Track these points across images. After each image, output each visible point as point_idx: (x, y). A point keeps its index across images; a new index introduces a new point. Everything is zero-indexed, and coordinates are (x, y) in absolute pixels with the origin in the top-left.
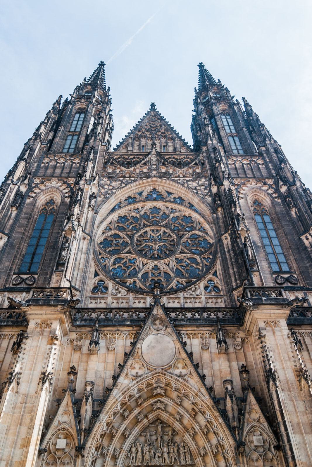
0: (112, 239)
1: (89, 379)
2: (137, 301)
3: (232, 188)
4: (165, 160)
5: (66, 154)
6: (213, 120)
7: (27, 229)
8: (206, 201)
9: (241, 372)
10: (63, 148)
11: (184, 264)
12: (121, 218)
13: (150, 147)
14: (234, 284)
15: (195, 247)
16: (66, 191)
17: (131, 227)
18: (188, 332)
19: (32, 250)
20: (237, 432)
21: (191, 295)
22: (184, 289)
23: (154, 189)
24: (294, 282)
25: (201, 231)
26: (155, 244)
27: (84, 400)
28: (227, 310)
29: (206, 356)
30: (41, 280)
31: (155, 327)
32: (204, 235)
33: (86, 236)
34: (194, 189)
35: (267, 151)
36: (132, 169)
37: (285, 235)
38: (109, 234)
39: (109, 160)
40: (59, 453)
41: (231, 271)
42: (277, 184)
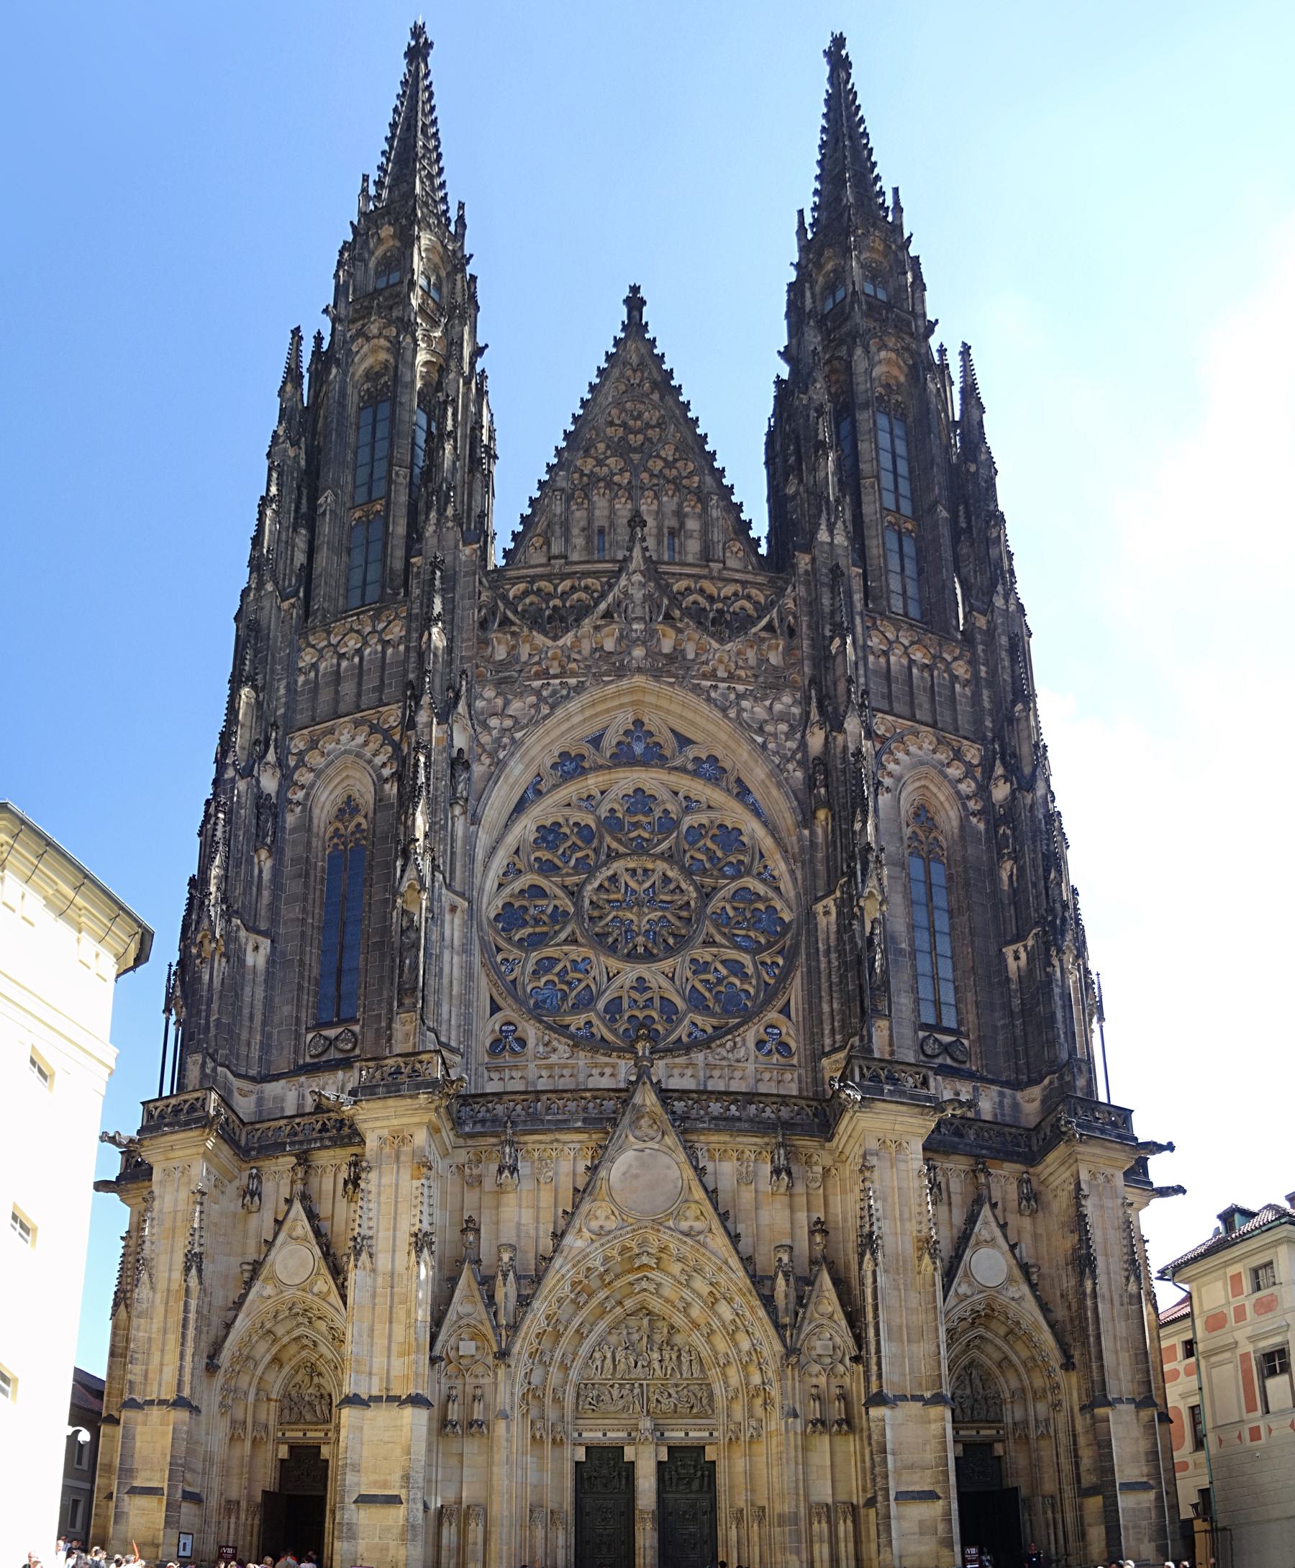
0: (525, 903)
1: (504, 1241)
2: (594, 1071)
9: (812, 1233)
12: (549, 835)
15: (741, 929)
20: (788, 1333)
21: (724, 1058)
25: (764, 881)
27: (500, 1277)
28: (803, 1103)
32: (771, 894)
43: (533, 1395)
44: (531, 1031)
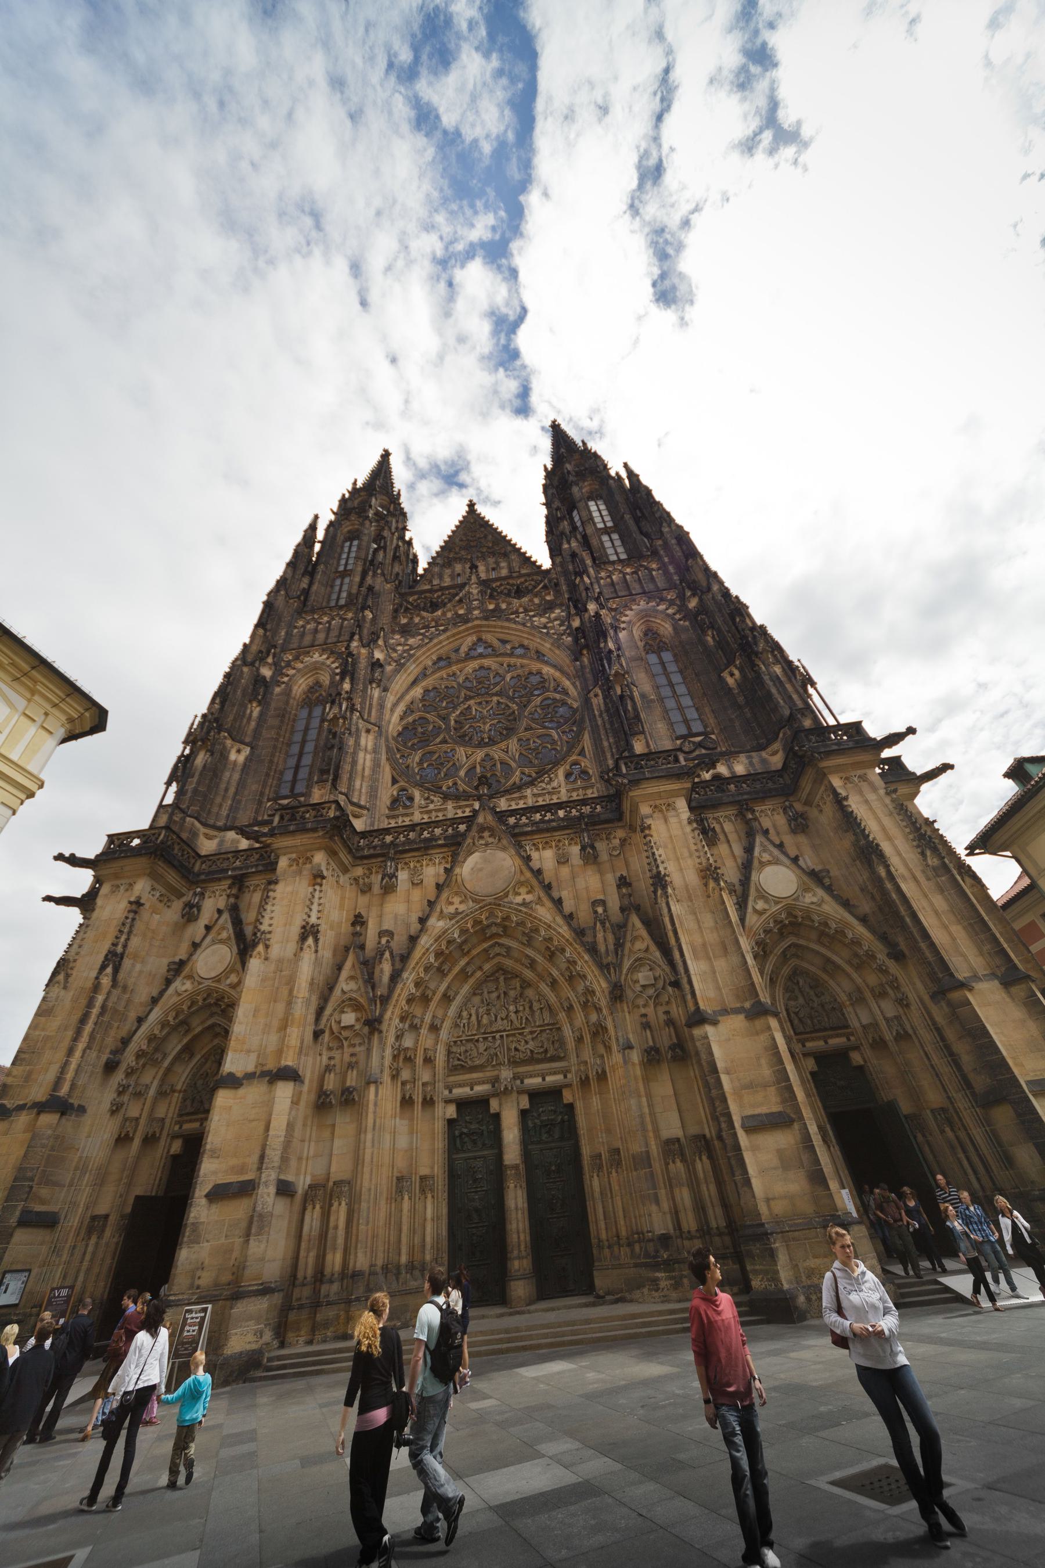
1: (385, 928)
2: (459, 811)
3: (603, 612)
4: (493, 590)
5: (331, 608)
6: (575, 513)
7: (282, 733)
9: (619, 887)
10: (329, 601)
11: (532, 746)
16: (337, 665)
17: (444, 704)
18: (535, 842)
19: (292, 762)
20: (612, 970)
22: (532, 783)
23: (480, 640)
24: (711, 746)
26: (484, 724)
28: (598, 801)
29: (565, 871)
31: (482, 842)
32: (563, 697)
33: (370, 727)
35: (666, 545)
36: (439, 613)
37: (696, 675)
38: (410, 719)
39: (401, 606)
40: (345, 1034)
41: (606, 744)
42: (682, 597)
43: (404, 1057)
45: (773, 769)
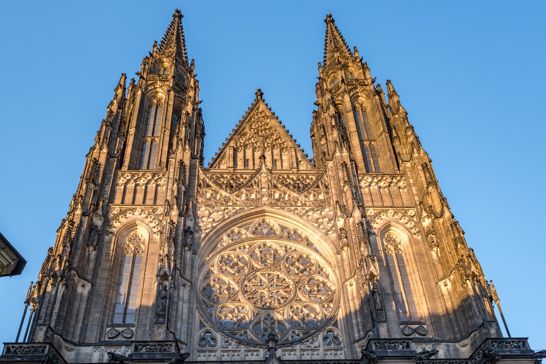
2: (249, 354)
8: (329, 238)
13: (257, 161)
14: (356, 335)
21: (309, 347)
24: (423, 333)
30: (140, 332)
34: (314, 222)
41: (354, 321)
44: (219, 336)
45: (462, 357)
